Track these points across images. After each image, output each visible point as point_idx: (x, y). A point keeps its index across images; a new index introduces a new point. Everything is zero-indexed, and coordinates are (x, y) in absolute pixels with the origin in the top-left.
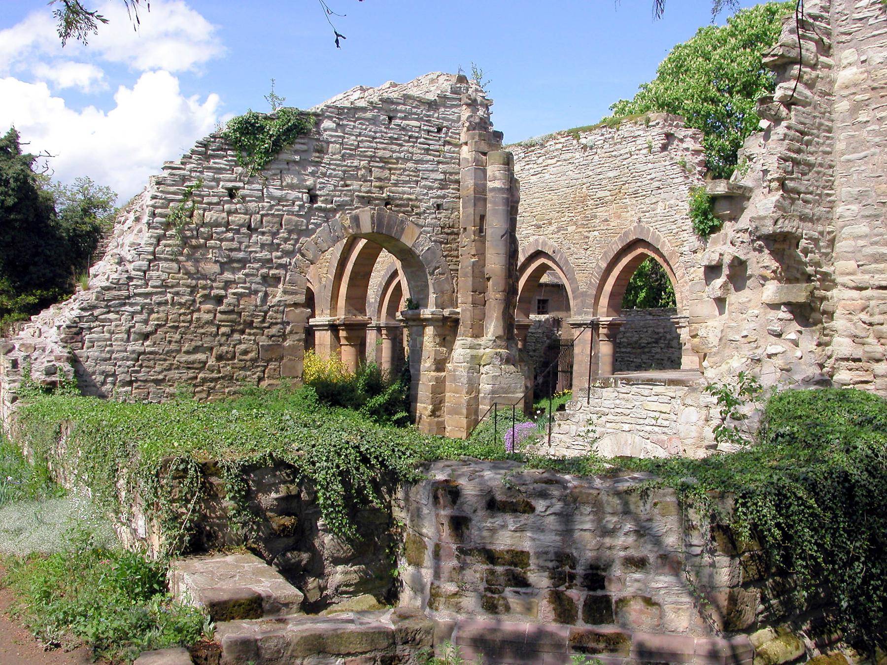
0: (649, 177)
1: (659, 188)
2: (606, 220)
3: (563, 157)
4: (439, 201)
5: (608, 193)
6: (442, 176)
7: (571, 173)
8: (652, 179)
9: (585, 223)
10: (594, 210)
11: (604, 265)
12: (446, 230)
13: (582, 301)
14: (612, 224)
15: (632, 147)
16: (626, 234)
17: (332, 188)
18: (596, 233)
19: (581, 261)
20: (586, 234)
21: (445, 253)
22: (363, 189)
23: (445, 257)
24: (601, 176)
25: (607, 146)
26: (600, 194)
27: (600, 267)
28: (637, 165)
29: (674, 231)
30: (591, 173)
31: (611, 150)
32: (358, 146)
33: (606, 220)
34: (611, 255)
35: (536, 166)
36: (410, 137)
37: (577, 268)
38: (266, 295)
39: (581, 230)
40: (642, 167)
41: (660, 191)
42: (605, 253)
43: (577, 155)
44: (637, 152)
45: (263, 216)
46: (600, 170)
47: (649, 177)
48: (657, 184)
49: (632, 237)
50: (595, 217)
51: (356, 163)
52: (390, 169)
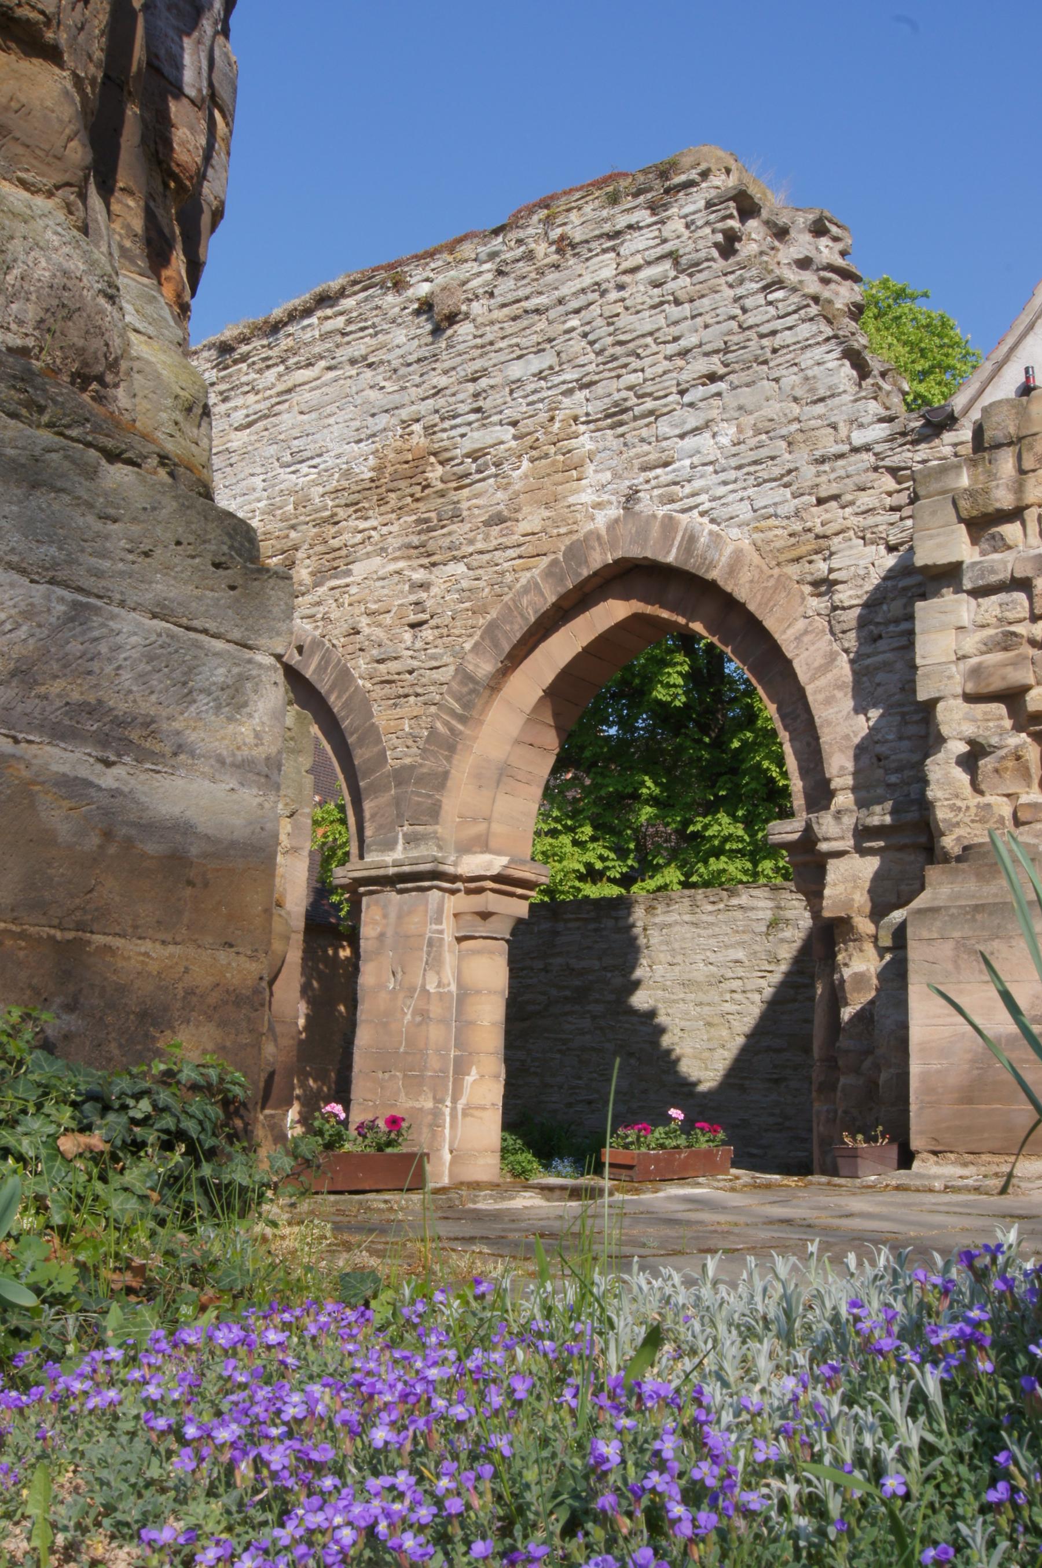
0: (671, 349)
1: (713, 378)
2: (498, 519)
3: (344, 354)
7: (373, 395)
8: (684, 353)
9: (415, 540)
10: (454, 496)
14: (524, 527)
15: (604, 268)
16: (576, 552)
19: (393, 666)
20: (419, 575)
24: (484, 383)
25: (506, 287)
26: (477, 438)
30: (443, 381)
31: (521, 293)
33: (498, 519)
34: (516, 630)
35: (252, 398)
37: (379, 692)
39: (401, 564)
40: (646, 322)
41: (713, 388)
42: (491, 629)
43: (400, 336)
44: (626, 279)
46: (478, 365)
47: (671, 349)
48: (701, 366)
49: (599, 558)
50: (456, 516)
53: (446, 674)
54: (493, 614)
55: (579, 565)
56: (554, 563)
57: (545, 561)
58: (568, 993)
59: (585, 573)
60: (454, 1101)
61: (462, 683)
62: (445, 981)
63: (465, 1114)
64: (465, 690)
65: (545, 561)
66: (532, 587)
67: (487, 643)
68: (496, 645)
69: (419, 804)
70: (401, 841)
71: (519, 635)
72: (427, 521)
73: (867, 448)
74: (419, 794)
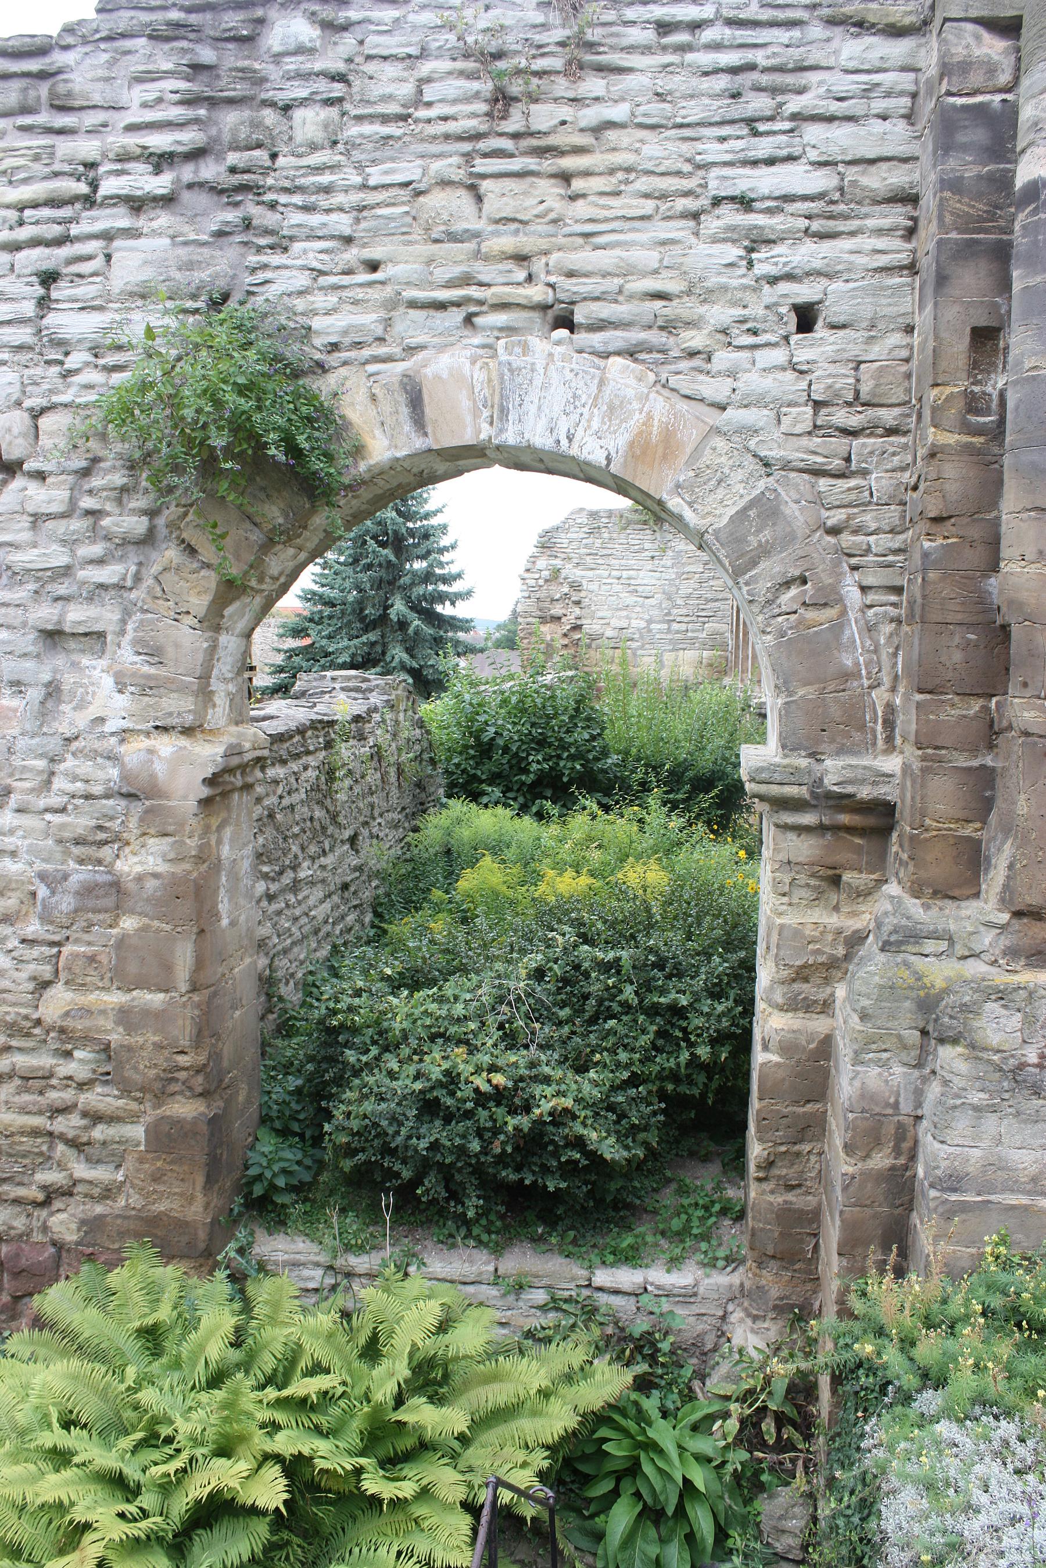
4: (805, 292)
6: (821, 181)
12: (841, 417)
17: (302, 280)
21: (836, 517)
22: (443, 274)
23: (834, 531)
32: (418, 100)
36: (664, 27)
38: (53, 691)
45: (36, 414)
51: (408, 170)
52: (565, 177)
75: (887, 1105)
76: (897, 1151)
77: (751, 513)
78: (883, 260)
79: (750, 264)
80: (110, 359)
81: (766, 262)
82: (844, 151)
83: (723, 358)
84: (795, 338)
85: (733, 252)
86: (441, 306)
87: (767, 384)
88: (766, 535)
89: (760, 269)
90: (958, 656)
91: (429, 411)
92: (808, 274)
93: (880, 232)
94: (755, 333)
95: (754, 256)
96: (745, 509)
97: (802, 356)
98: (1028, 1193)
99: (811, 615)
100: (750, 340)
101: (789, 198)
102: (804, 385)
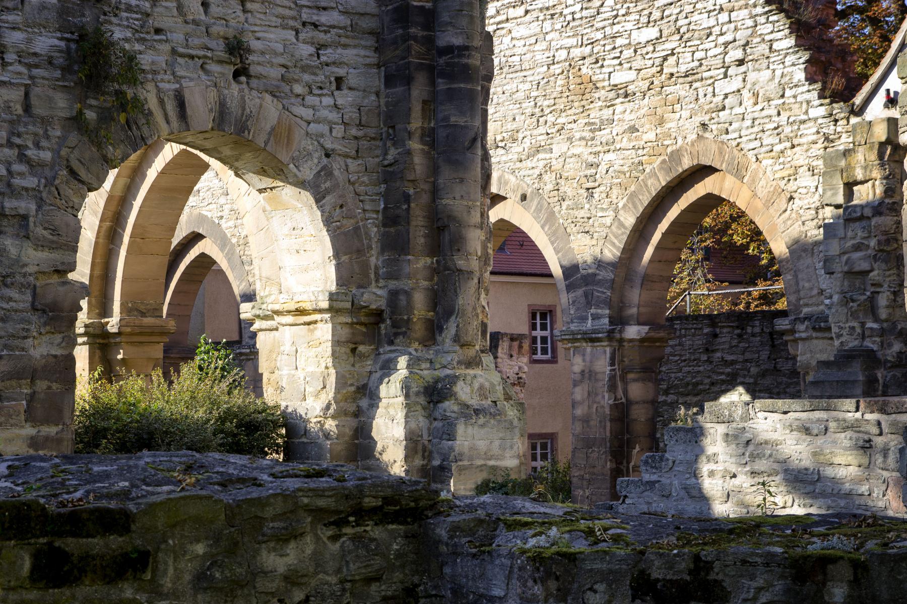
0: (721, 40)
2: (633, 129)
4: (341, 72)
5: (632, 75)
6: (344, 21)
9: (588, 135)
11: (630, 220)
13: (586, 295)
14: (646, 137)
16: (676, 156)
18: (611, 156)
20: (591, 159)
26: (620, 77)
27: (621, 225)
28: (695, 17)
29: (778, 148)
30: (599, 35)
34: (645, 199)
47: (721, 40)
48: (738, 54)
49: (687, 163)
53: (608, 221)
54: (633, 188)
55: (677, 165)
56: (664, 161)
57: (661, 159)
58: (723, 377)
59: (681, 170)
60: (628, 463)
61: (618, 228)
62: (619, 397)
63: (633, 471)
64: (620, 232)
65: (661, 159)
66: (653, 174)
67: (630, 205)
68: (635, 207)
69: (598, 297)
70: (590, 318)
71: (647, 203)
72: (593, 124)
73: (816, 119)
74: (598, 291)
75: (419, 436)
76: (424, 457)
77: (322, 173)
78: (368, 61)
79: (318, 57)
80: (31, 60)
81: (327, 55)
82: (353, 8)
83: (310, 99)
84: (336, 93)
85: (312, 50)
86: (192, 57)
87: (325, 113)
88: (328, 184)
89: (323, 59)
90: (422, 240)
91: (189, 112)
92: (340, 63)
93: (365, 47)
94: (321, 88)
95: (320, 52)
96: (319, 172)
97: (340, 102)
98: (484, 459)
99: (345, 222)
100: (320, 92)
101: (334, 27)
102: (340, 115)
